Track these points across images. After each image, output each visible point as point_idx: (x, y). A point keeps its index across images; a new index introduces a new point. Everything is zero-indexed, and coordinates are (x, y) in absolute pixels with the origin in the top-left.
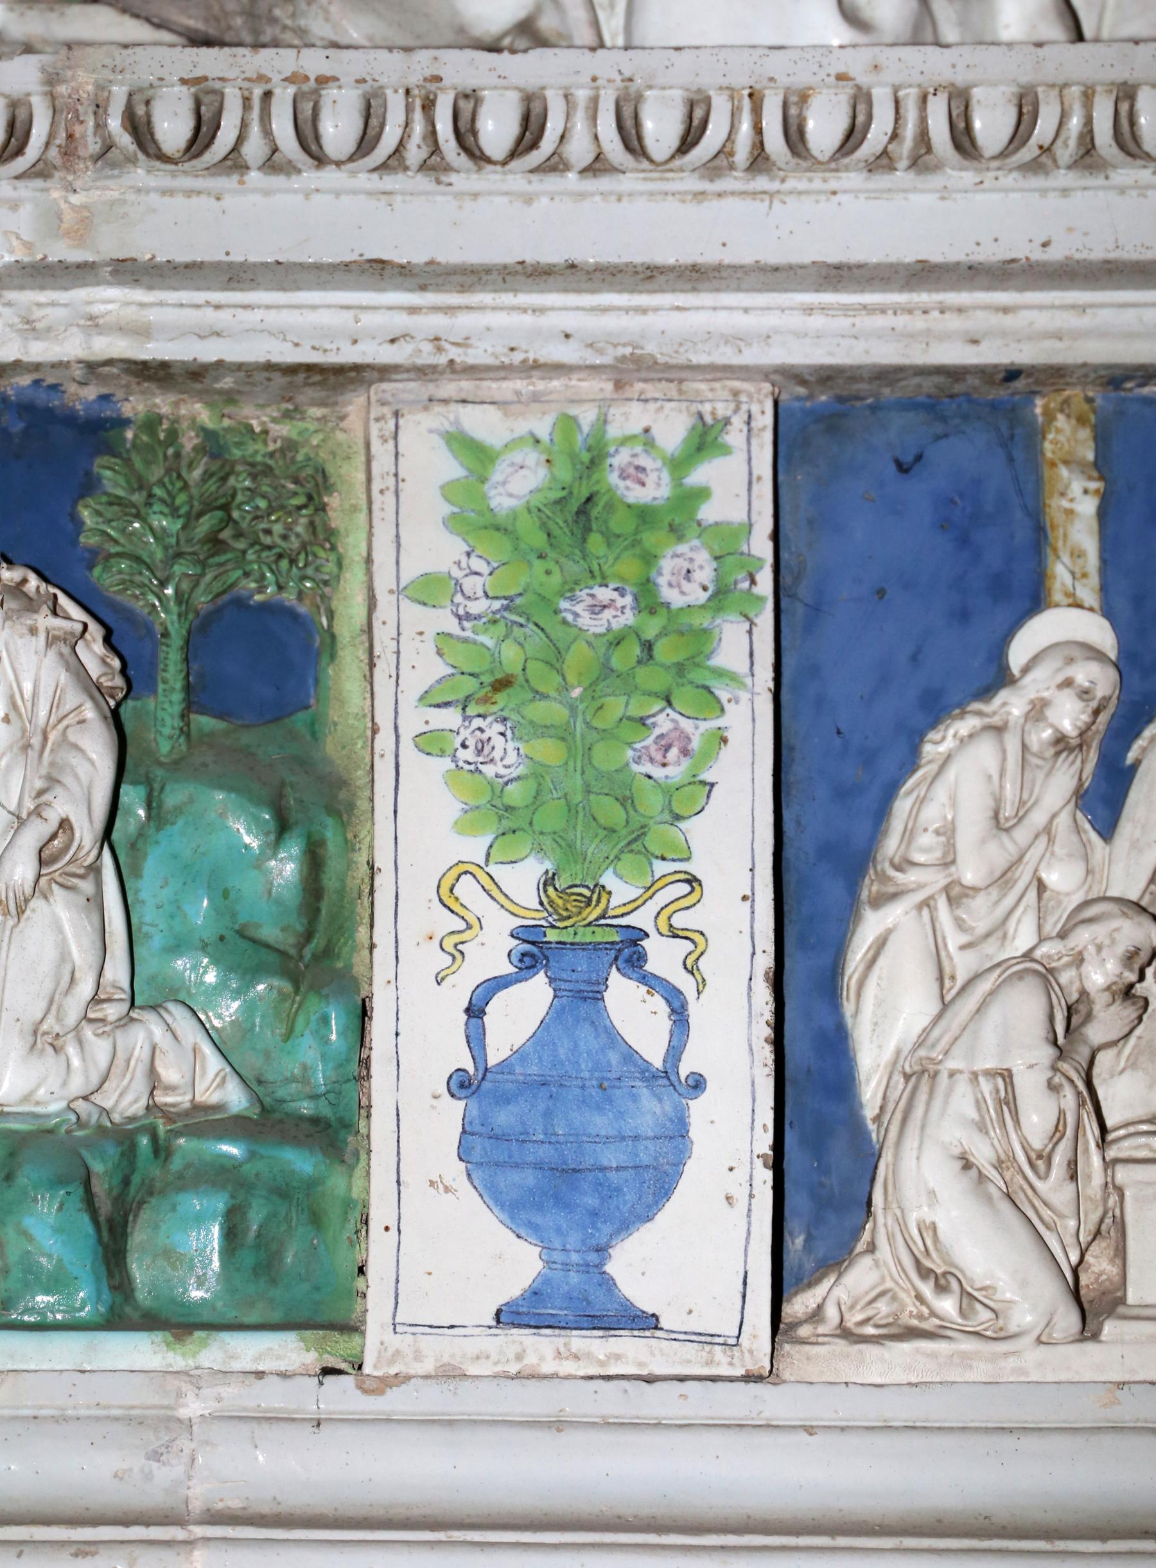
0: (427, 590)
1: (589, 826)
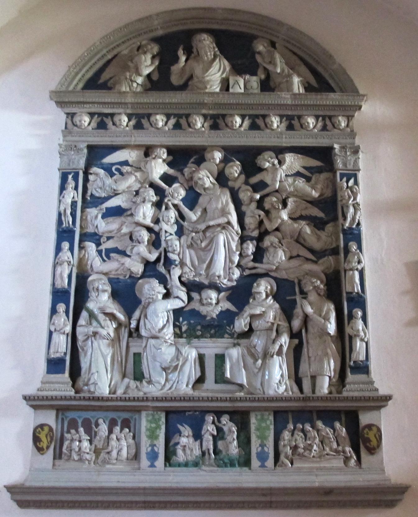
0: (254, 423)
1: (262, 438)
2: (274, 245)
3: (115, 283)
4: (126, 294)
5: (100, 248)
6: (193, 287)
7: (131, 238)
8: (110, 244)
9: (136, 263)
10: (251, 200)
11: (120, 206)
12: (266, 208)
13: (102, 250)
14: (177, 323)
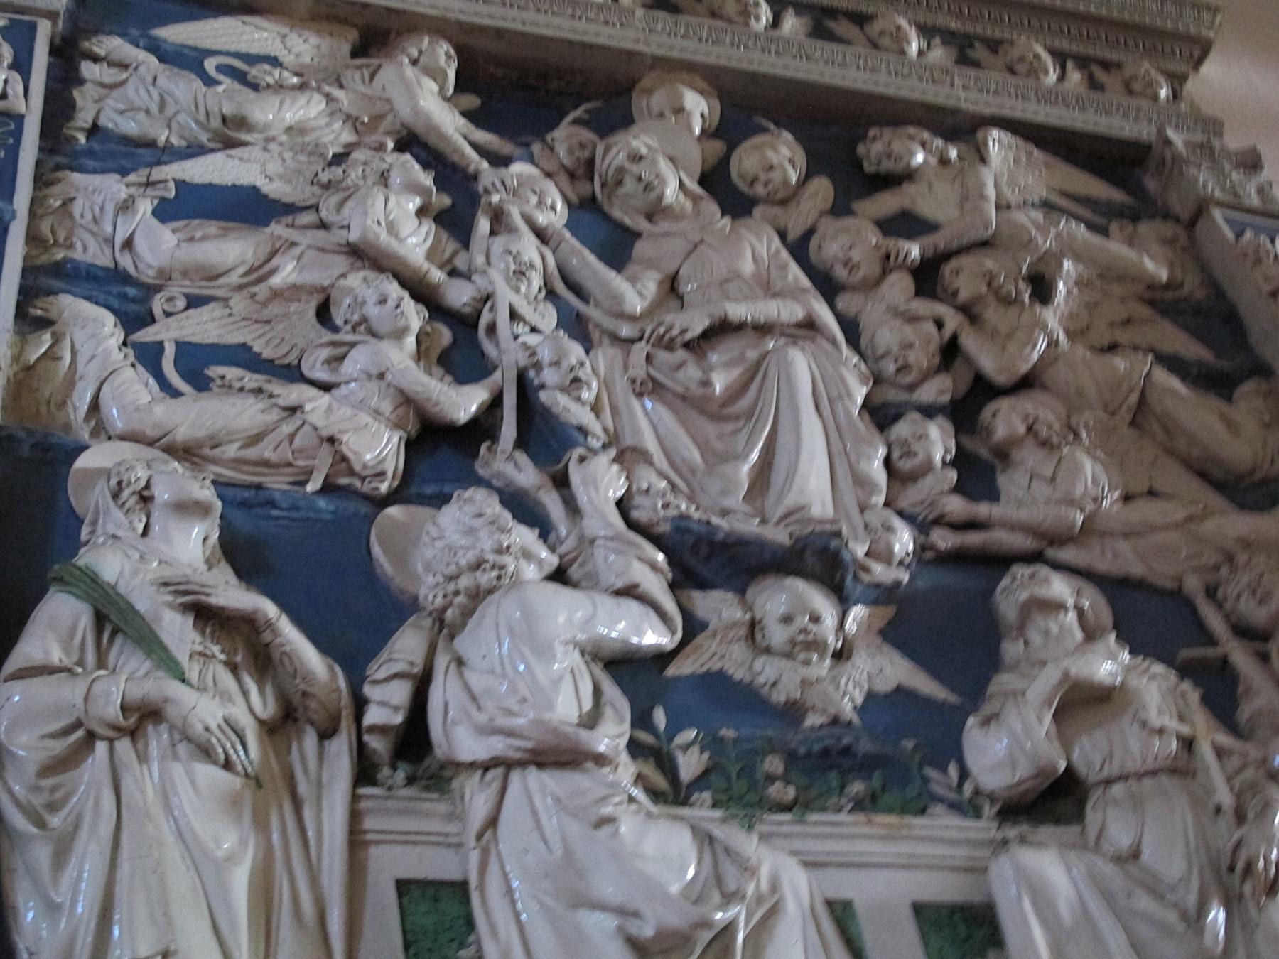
2: (1044, 432)
3: (244, 505)
4: (312, 562)
5: (146, 335)
6: (703, 560)
7: (323, 314)
8: (204, 327)
9: (365, 418)
10: (887, 263)
11: (255, 190)
12: (964, 295)
13: (160, 346)
14: (645, 737)
